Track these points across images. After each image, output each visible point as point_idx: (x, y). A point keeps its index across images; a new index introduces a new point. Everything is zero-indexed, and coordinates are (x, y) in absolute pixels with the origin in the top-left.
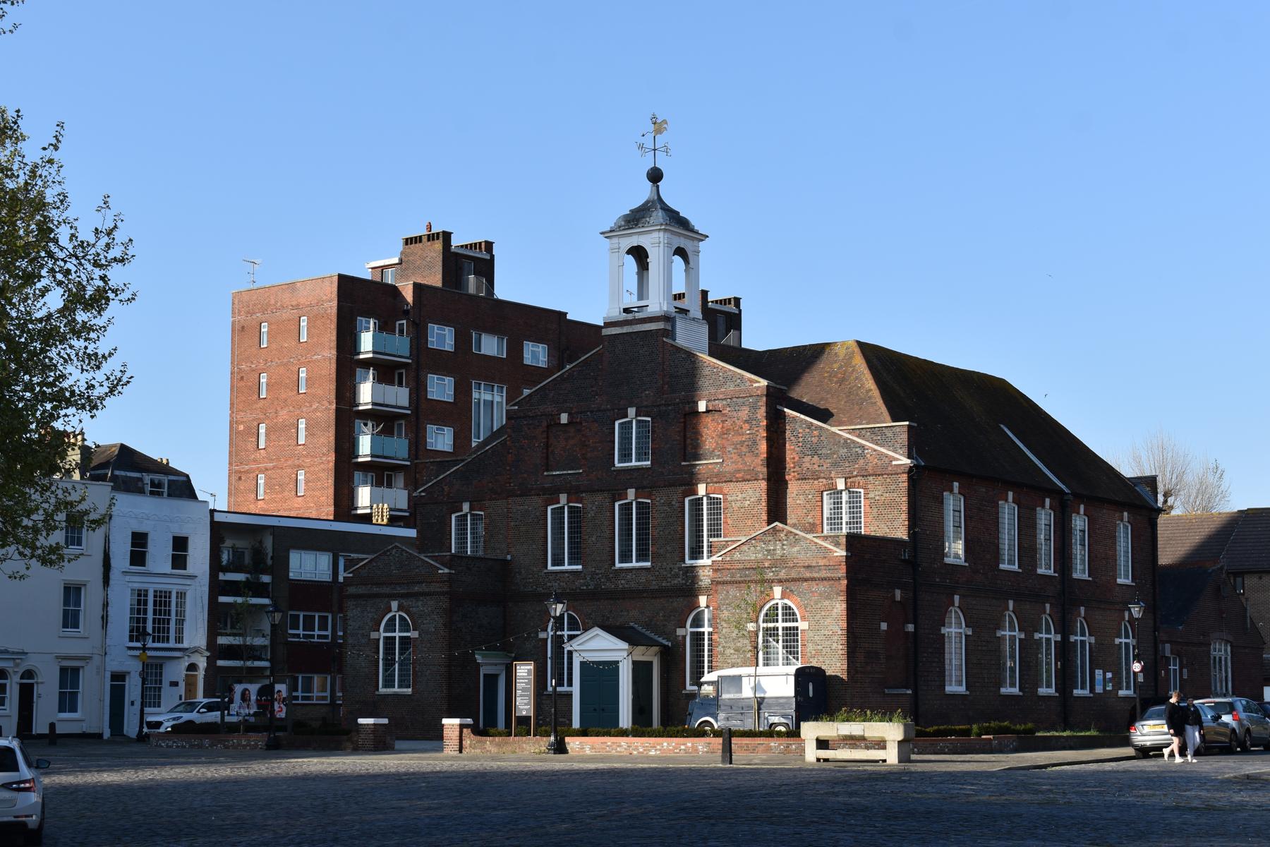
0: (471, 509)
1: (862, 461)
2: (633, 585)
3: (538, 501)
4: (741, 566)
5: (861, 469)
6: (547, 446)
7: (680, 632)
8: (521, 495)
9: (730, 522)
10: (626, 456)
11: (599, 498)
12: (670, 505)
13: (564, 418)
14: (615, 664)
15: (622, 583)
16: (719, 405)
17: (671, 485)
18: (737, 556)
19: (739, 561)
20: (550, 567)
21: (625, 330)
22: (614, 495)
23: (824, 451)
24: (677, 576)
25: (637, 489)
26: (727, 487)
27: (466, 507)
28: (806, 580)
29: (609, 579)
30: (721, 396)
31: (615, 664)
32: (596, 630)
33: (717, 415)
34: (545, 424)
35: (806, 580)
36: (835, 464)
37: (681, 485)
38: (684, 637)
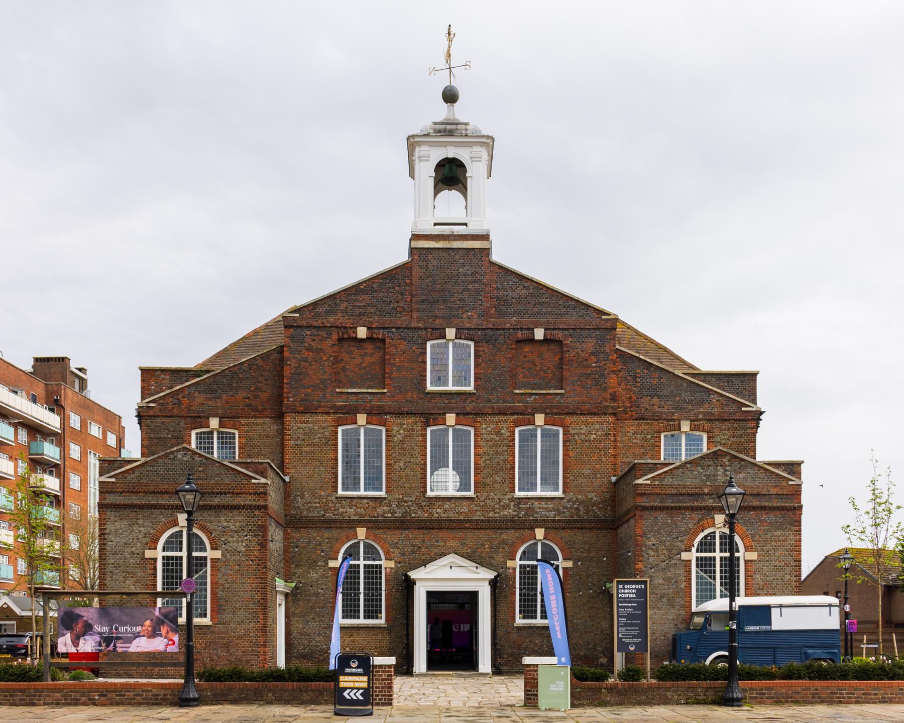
0: (221, 425)
1: (707, 405)
2: (452, 515)
3: (329, 419)
4: (674, 491)
5: (704, 413)
7: (510, 564)
8: (302, 413)
9: (571, 454)
10: (440, 379)
11: (409, 421)
12: (498, 433)
14: (474, 595)
15: (437, 512)
16: (560, 335)
17: (503, 413)
18: (668, 481)
19: (671, 486)
20: (340, 492)
23: (665, 393)
24: (507, 507)
25: (457, 414)
26: (568, 420)
27: (214, 423)
28: (754, 508)
29: (421, 507)
31: (474, 595)
33: (553, 346)
34: (335, 336)
35: (754, 508)
36: (677, 407)
37: (511, 414)
38: (514, 569)
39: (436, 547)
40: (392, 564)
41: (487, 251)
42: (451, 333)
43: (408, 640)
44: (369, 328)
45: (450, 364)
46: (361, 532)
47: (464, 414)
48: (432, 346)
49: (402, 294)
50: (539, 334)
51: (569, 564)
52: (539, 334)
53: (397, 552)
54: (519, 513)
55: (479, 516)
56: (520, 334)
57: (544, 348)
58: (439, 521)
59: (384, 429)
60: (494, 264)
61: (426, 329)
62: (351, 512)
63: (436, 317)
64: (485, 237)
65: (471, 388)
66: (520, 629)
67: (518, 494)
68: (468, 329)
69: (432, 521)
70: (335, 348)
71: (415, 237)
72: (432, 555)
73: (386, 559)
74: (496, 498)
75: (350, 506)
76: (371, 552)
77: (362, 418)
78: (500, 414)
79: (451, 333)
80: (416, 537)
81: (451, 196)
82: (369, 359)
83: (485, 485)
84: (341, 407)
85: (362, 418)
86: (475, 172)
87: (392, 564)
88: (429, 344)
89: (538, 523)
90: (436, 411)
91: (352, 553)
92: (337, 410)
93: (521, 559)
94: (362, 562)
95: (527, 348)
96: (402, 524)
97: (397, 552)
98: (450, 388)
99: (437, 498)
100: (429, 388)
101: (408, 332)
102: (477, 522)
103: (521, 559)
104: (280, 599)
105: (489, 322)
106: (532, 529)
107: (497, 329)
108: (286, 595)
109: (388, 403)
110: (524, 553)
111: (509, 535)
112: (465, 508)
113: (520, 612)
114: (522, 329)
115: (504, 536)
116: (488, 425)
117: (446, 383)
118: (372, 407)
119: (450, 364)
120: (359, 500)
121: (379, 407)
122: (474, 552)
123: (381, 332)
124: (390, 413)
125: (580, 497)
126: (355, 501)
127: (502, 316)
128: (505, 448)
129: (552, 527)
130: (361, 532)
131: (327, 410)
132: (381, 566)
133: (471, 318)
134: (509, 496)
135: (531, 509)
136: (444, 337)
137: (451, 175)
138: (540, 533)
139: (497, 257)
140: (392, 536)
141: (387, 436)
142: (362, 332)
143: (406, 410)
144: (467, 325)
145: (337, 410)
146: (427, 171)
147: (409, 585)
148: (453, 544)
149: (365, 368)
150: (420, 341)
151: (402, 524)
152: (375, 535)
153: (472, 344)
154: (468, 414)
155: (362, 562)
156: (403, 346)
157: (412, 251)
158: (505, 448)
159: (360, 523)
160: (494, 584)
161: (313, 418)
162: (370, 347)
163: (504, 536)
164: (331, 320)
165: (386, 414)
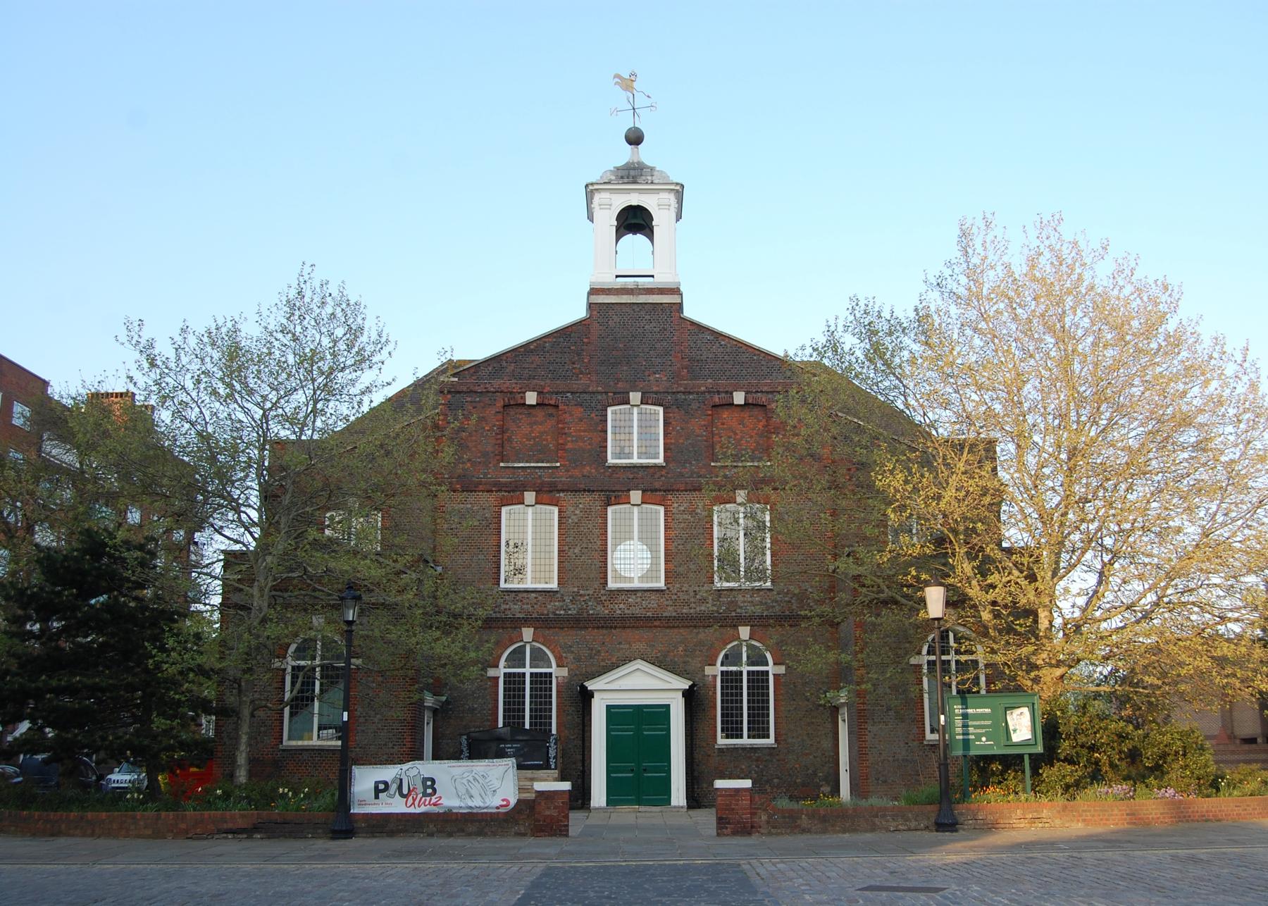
2: (637, 611)
3: (488, 499)
6: (503, 430)
7: (709, 670)
11: (585, 500)
13: (531, 398)
15: (620, 608)
16: (763, 399)
21: (642, 299)
22: (609, 498)
24: (704, 600)
25: (644, 491)
29: (600, 602)
30: (765, 389)
32: (639, 664)
33: (756, 411)
34: (500, 404)
38: (715, 677)
39: (619, 650)
40: (564, 672)
41: (680, 306)
42: (635, 397)
43: (583, 766)
44: (540, 393)
45: (636, 434)
46: (528, 633)
47: (652, 491)
48: (614, 413)
49: (579, 355)
50: (739, 398)
51: (781, 670)
52: (739, 398)
53: (571, 656)
54: (720, 607)
55: (670, 612)
56: (716, 399)
57: (746, 414)
58: (623, 618)
59: (556, 510)
60: (685, 319)
61: (606, 393)
62: (516, 609)
63: (619, 380)
64: (676, 291)
65: (660, 460)
66: (721, 751)
67: (719, 584)
68: (656, 393)
69: (613, 619)
70: (500, 416)
71: (593, 291)
72: (614, 660)
73: (558, 666)
74: (691, 590)
75: (515, 602)
76: (538, 658)
77: (530, 497)
78: (695, 490)
79: (635, 397)
80: (593, 637)
81: (635, 241)
82: (538, 428)
83: (678, 575)
84: (505, 484)
85: (530, 497)
86: (661, 219)
87: (564, 672)
88: (610, 410)
89: (743, 620)
90: (617, 488)
91: (517, 658)
92: (500, 487)
93: (722, 665)
94: (528, 670)
95: (725, 414)
96: (578, 622)
97: (571, 656)
98: (635, 460)
99: (620, 591)
100: (611, 461)
101: (587, 397)
102: (668, 619)
103: (722, 665)
104: (427, 716)
105: (680, 385)
106: (735, 627)
107: (690, 393)
108: (435, 712)
109: (563, 478)
110: (726, 656)
111: (706, 635)
112: (653, 602)
113: (723, 730)
114: (719, 392)
115: (702, 636)
116: (680, 503)
117: (630, 455)
118: (543, 483)
119: (636, 434)
120: (525, 595)
121: (549, 483)
122: (665, 656)
123: (554, 396)
124: (563, 491)
125: (792, 588)
126: (520, 595)
127: (695, 378)
128: (701, 531)
129: (759, 623)
130: (528, 633)
131: (488, 487)
132: (551, 674)
133: (659, 380)
134: (706, 587)
135: (733, 603)
136: (627, 402)
137: (635, 221)
138: (744, 632)
139: (690, 312)
140: (567, 637)
141: (560, 517)
142: (531, 398)
143: (582, 486)
144: (655, 389)
145: (500, 487)
146: (607, 220)
147: (586, 697)
148: (641, 646)
149: (534, 438)
150: (599, 407)
151: (578, 622)
152: (544, 637)
153: (661, 410)
154: (656, 490)
155: (528, 670)
156: (578, 412)
157: (591, 306)
158: (701, 531)
159: (526, 622)
160: (689, 695)
161: (472, 497)
162: (540, 414)
163: (702, 636)
164: (497, 383)
165: (559, 491)
